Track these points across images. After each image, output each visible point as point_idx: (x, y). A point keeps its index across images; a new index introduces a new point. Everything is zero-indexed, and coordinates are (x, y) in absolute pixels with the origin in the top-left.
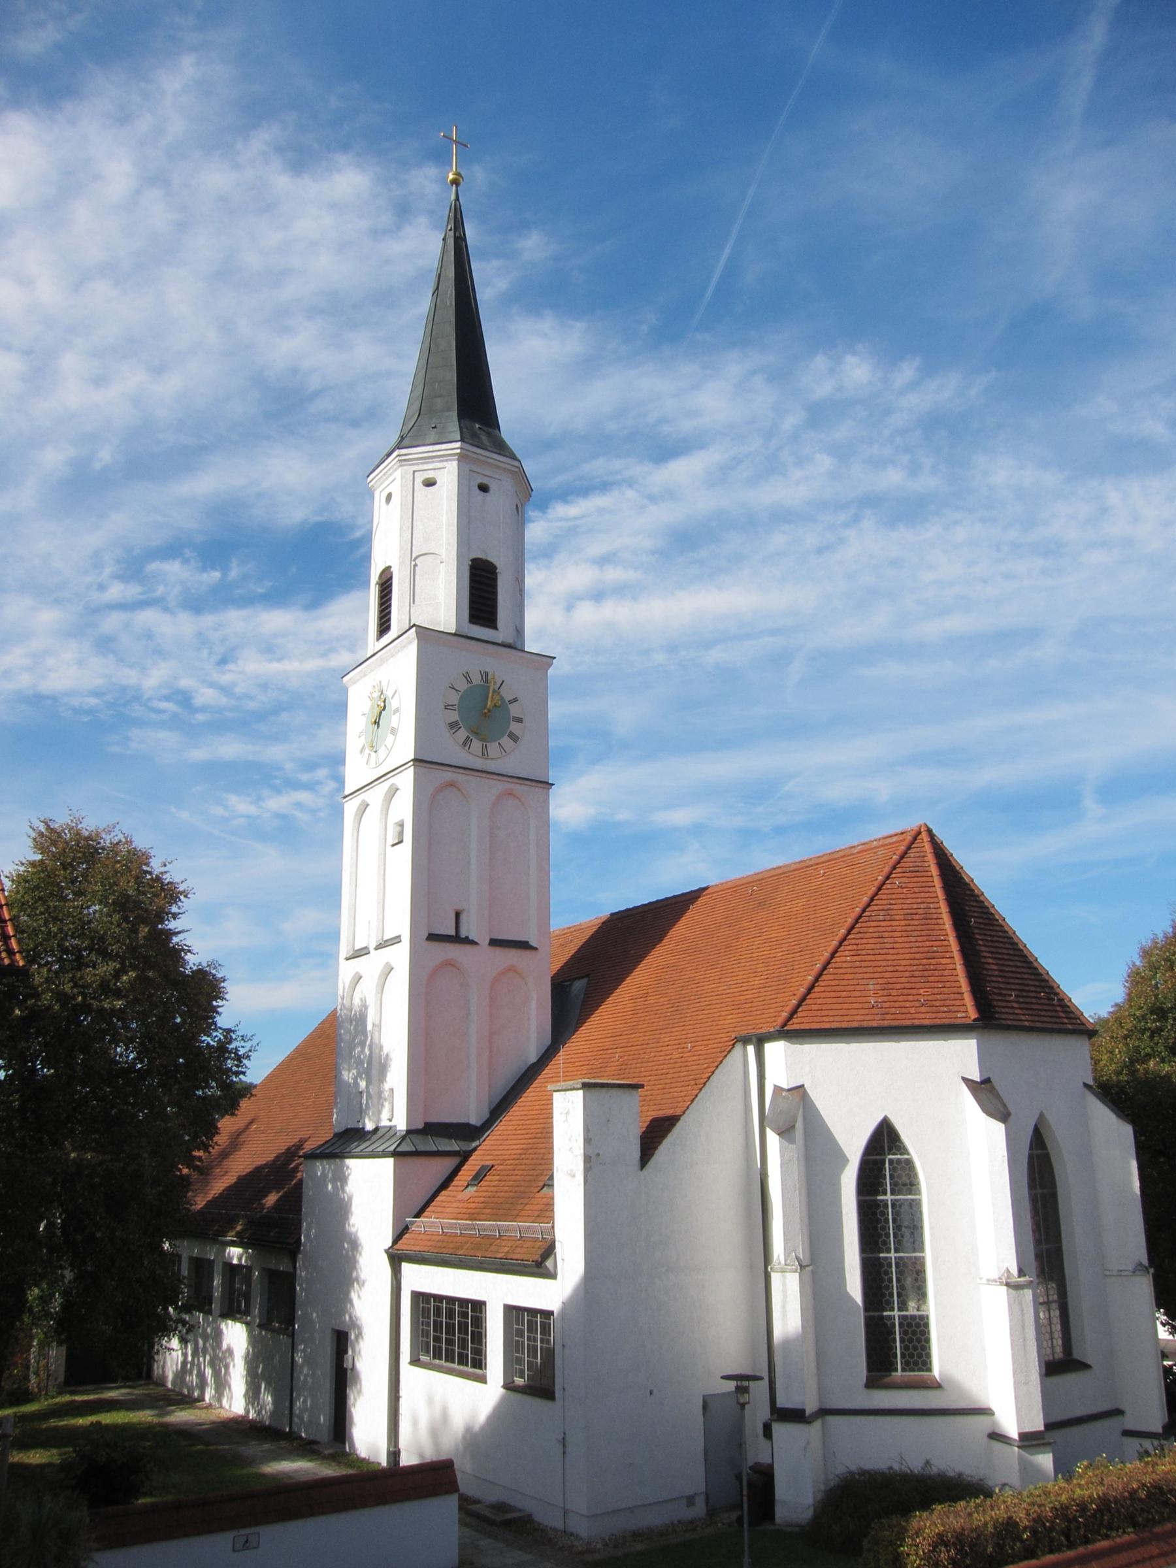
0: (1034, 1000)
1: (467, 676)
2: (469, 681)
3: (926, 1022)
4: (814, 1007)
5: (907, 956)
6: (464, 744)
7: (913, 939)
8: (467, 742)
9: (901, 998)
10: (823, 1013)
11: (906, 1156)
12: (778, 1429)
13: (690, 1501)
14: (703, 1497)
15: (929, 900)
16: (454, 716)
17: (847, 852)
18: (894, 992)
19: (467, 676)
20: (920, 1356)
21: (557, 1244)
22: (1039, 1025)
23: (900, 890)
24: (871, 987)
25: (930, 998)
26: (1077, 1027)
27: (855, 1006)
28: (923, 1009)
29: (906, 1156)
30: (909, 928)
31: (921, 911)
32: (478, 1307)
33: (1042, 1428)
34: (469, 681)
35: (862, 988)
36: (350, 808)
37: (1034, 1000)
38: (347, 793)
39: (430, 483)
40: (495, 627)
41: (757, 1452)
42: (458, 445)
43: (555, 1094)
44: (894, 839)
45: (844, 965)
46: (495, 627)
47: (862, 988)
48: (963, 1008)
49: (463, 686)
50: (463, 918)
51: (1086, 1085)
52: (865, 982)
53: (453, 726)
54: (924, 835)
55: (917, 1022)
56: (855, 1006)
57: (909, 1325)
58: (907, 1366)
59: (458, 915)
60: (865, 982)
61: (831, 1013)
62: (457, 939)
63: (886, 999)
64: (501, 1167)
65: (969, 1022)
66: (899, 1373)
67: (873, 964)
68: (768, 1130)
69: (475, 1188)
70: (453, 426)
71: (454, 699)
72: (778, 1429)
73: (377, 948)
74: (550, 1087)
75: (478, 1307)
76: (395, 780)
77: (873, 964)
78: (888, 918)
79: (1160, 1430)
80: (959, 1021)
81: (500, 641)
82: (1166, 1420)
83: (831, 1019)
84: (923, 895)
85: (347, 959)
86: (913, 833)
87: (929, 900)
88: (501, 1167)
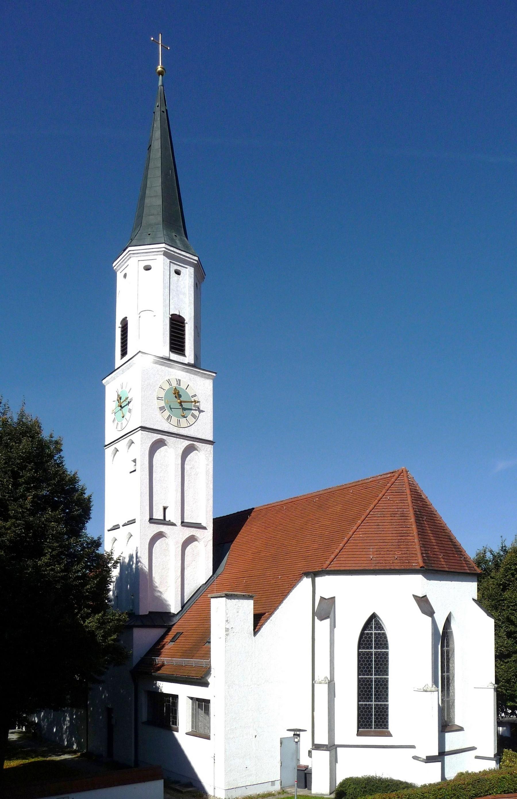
0: (452, 558)
1: (169, 381)
2: (170, 384)
3: (397, 568)
4: (342, 559)
5: (390, 535)
6: (168, 419)
7: (395, 526)
8: (169, 418)
9: (386, 556)
10: (347, 562)
11: (383, 632)
12: (314, 752)
13: (273, 783)
14: (279, 782)
15: (403, 507)
16: (162, 404)
17: (364, 482)
18: (382, 553)
19: (169, 381)
20: (383, 722)
21: (212, 670)
22: (452, 570)
23: (389, 502)
24: (371, 550)
25: (400, 556)
26: (472, 572)
27: (363, 559)
28: (396, 561)
29: (383, 632)
30: (393, 521)
31: (399, 513)
32: (175, 697)
33: (437, 754)
34: (170, 384)
35: (367, 550)
36: (109, 452)
37: (452, 558)
38: (106, 444)
39: (148, 268)
40: (184, 355)
41: (304, 761)
42: (163, 245)
43: (212, 599)
44: (389, 475)
45: (358, 539)
46: (184, 355)
47: (367, 550)
48: (416, 561)
49: (167, 387)
50: (167, 511)
51: (473, 599)
52: (369, 547)
53: (162, 409)
54: (405, 472)
55: (392, 568)
56: (363, 559)
57: (379, 708)
58: (377, 726)
59: (165, 509)
60: (369, 547)
61: (350, 562)
62: (164, 522)
63: (378, 556)
64: (186, 633)
65: (418, 568)
66: (373, 729)
67: (373, 538)
68: (316, 618)
69: (174, 643)
70: (161, 233)
71: (162, 394)
72: (314, 752)
73: (123, 526)
74: (209, 596)
75: (175, 697)
76: (132, 437)
77: (373, 538)
78: (382, 516)
79: (493, 757)
80: (413, 568)
81: (186, 363)
82: (496, 752)
83: (350, 565)
84: (401, 504)
85: (109, 531)
86: (399, 473)
87: (403, 507)
88: (186, 633)
